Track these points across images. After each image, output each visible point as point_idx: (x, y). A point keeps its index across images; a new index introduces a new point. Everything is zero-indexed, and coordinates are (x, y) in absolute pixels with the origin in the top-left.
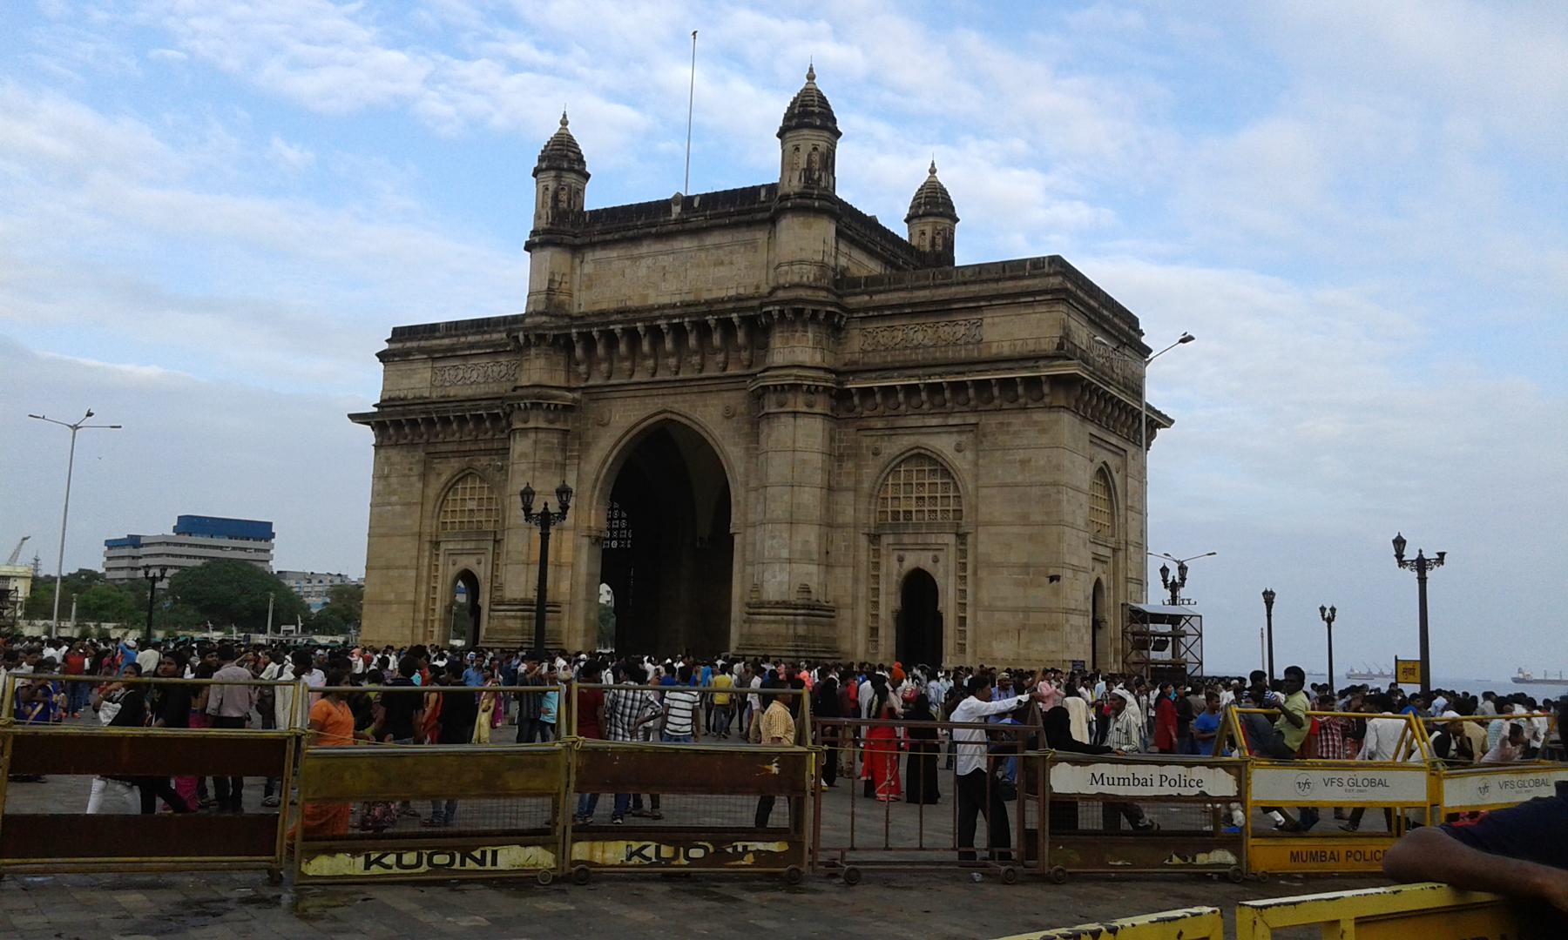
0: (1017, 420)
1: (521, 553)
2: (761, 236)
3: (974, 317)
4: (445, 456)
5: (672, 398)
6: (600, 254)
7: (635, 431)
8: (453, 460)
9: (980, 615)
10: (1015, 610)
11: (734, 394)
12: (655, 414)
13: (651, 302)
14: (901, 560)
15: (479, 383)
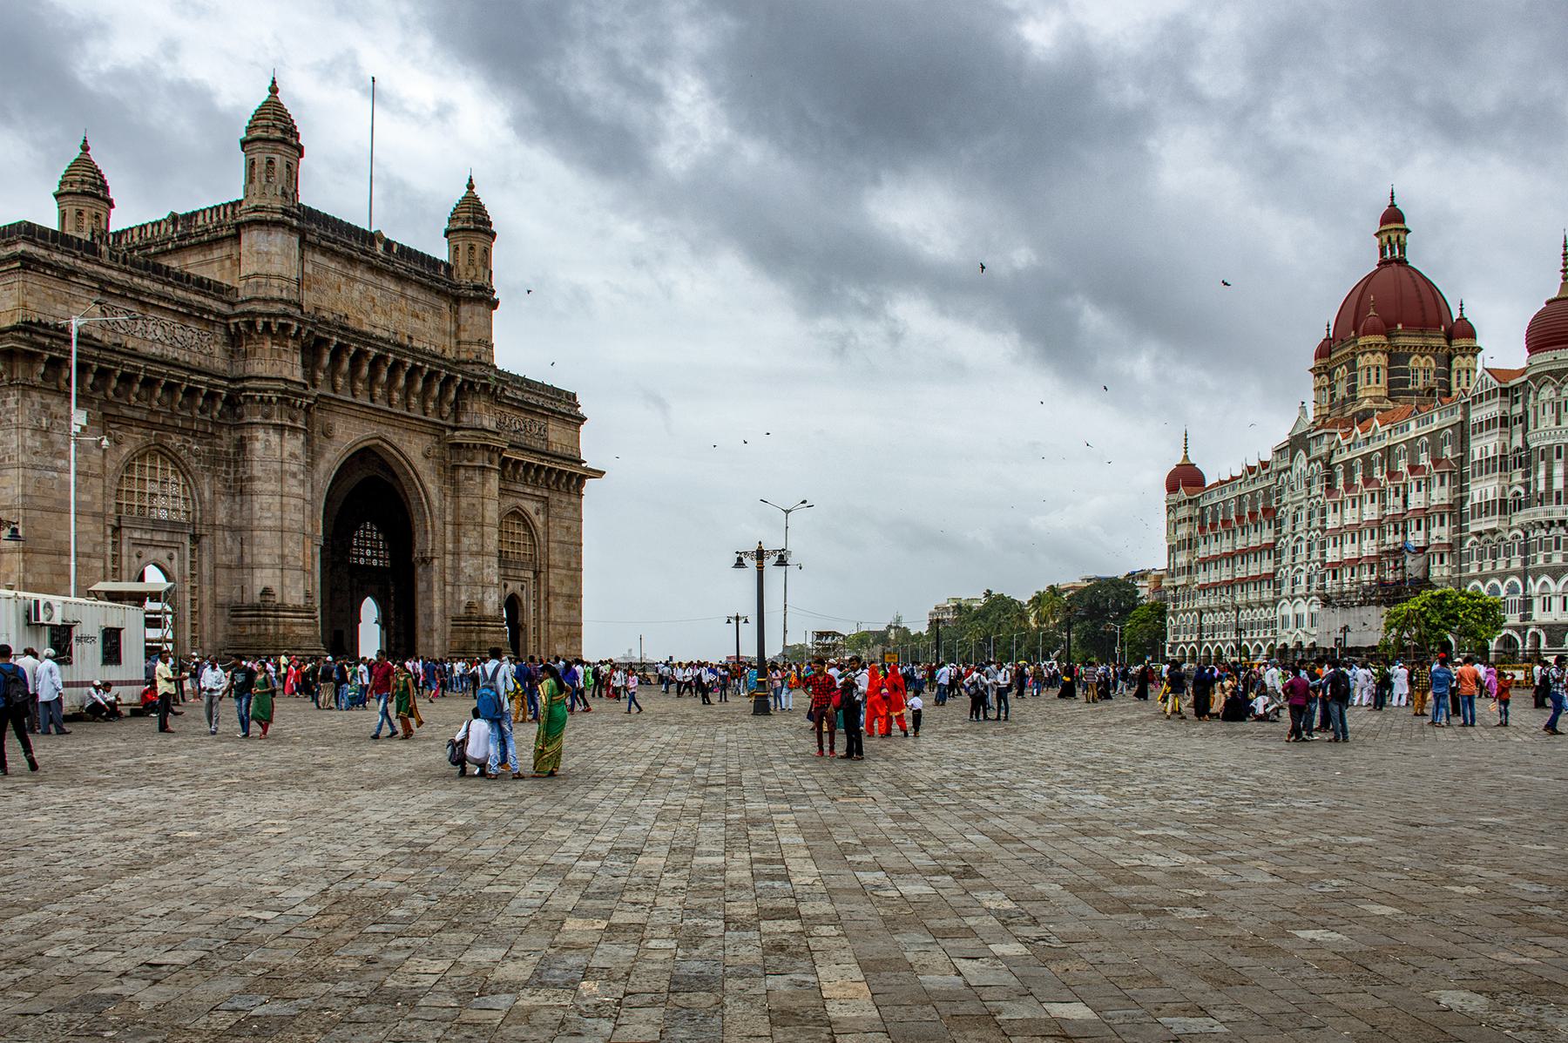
0: (565, 499)
1: (297, 558)
2: (445, 306)
3: (543, 421)
4: (127, 423)
5: (385, 428)
6: (318, 258)
7: (353, 450)
8: (135, 429)
9: (551, 626)
10: (564, 624)
11: (429, 437)
12: (371, 439)
13: (366, 328)
14: (506, 586)
15: (163, 343)
